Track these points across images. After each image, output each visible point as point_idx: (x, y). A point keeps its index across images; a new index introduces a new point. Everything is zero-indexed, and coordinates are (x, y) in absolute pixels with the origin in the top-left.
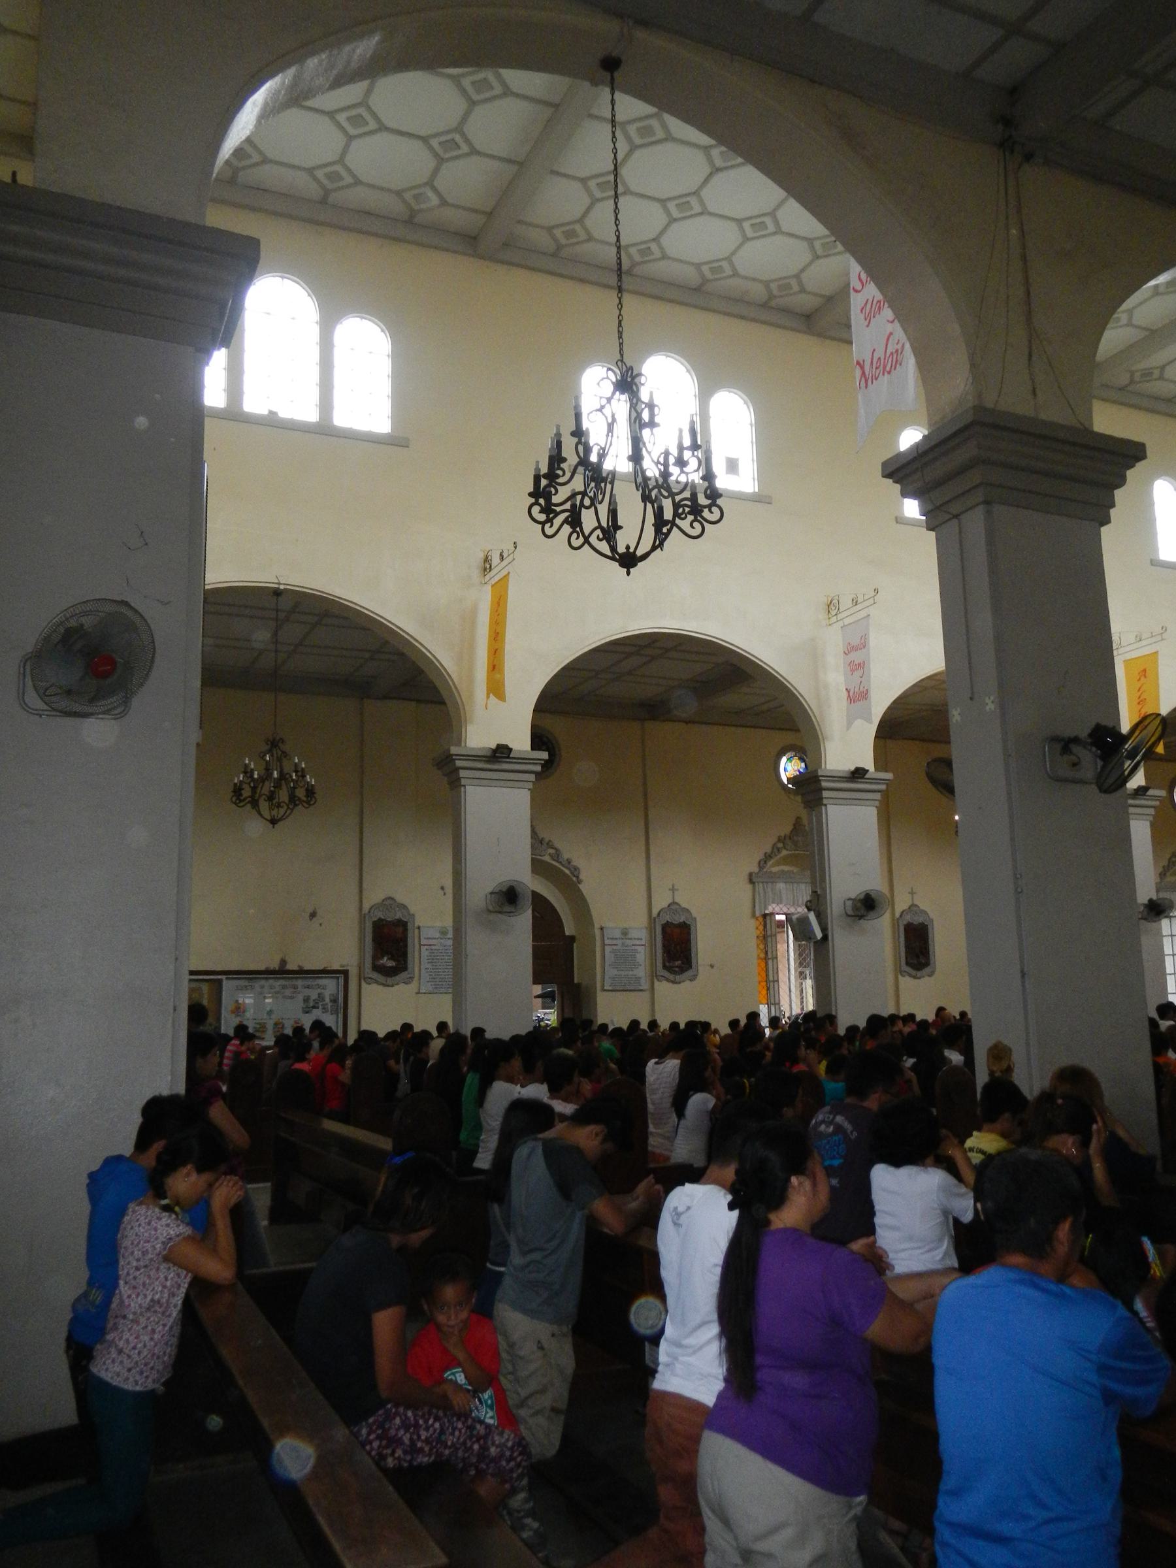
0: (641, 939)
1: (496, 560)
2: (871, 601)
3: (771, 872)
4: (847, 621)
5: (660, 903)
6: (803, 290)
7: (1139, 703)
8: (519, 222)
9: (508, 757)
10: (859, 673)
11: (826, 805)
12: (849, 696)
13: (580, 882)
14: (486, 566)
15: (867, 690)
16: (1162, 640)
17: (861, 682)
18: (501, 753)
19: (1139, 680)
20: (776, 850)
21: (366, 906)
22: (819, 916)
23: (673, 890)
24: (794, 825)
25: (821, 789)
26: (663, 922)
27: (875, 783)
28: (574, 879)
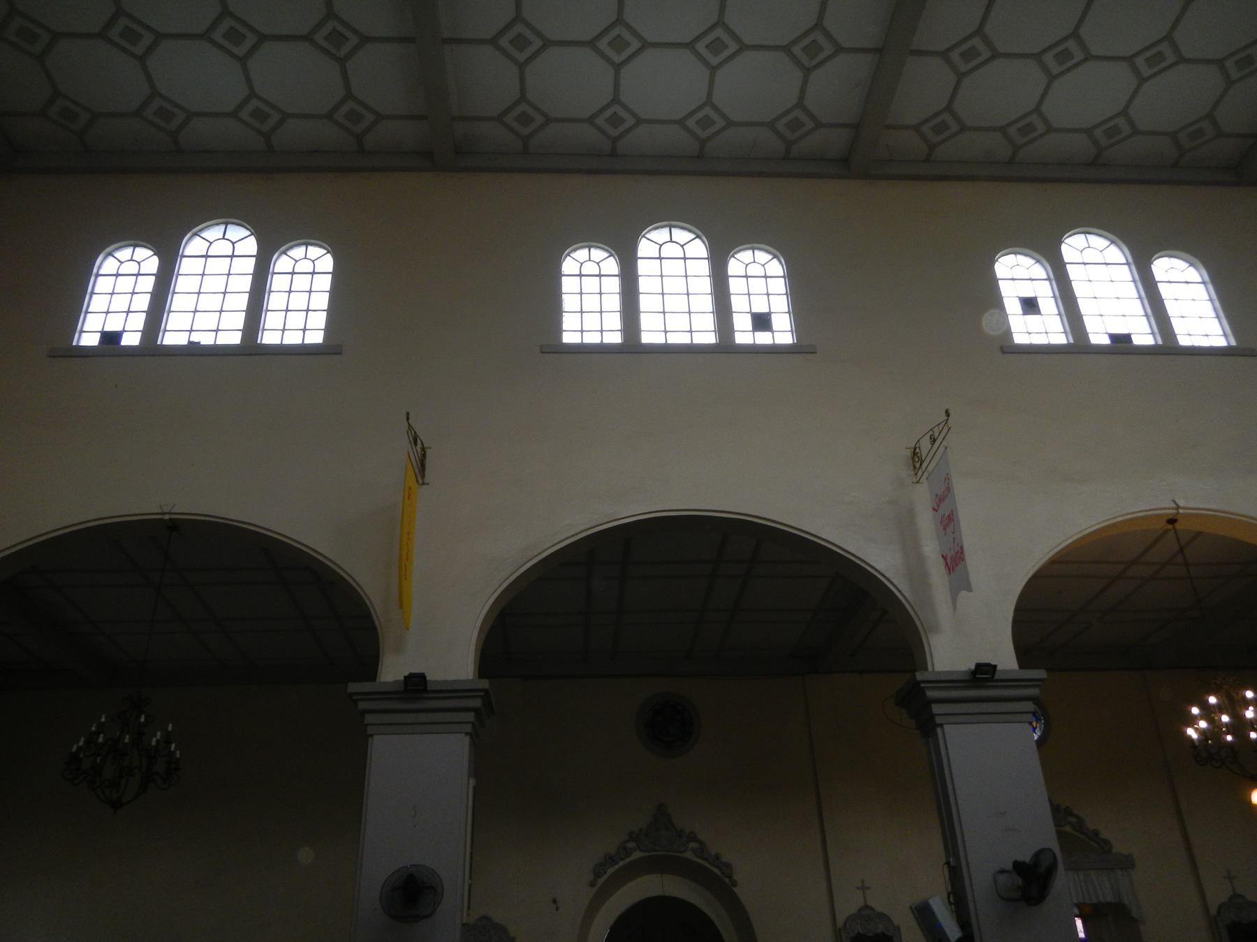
5: (848, 906)
11: (941, 725)
12: (947, 563)
13: (734, 884)
23: (863, 888)
25: (930, 702)
27: (1026, 686)
28: (727, 880)
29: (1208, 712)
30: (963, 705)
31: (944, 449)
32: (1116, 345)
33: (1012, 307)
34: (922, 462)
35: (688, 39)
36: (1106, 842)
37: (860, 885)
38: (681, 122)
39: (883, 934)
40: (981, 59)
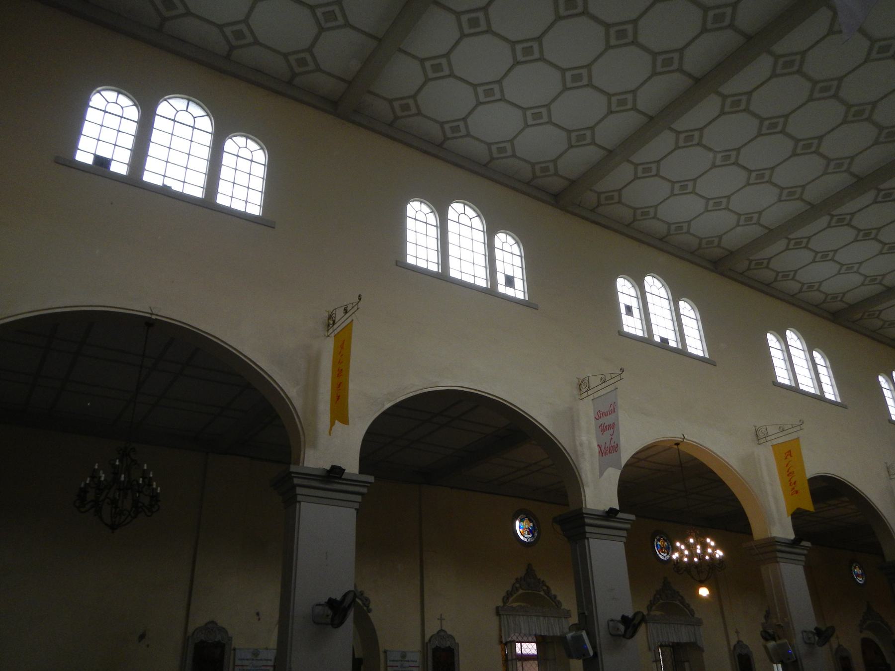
0: (416, 661)
1: (339, 314)
2: (618, 378)
3: (512, 607)
4: (596, 395)
5: (432, 629)
6: (556, 174)
7: (788, 475)
8: (370, 92)
9: (340, 478)
10: (611, 431)
12: (601, 450)
13: (370, 611)
14: (331, 321)
15: (617, 444)
16: (801, 429)
17: (612, 439)
18: (336, 472)
19: (786, 458)
20: (514, 589)
21: (190, 630)
22: (588, 634)
24: (527, 570)
26: (434, 647)
28: (365, 608)
29: (689, 547)
30: (593, 528)
31: (614, 388)
32: (661, 343)
33: (623, 310)
34: (589, 389)
35: (476, 82)
36: (559, 602)
37: (439, 618)
38: (285, 56)
39: (449, 647)
40: (542, 121)
